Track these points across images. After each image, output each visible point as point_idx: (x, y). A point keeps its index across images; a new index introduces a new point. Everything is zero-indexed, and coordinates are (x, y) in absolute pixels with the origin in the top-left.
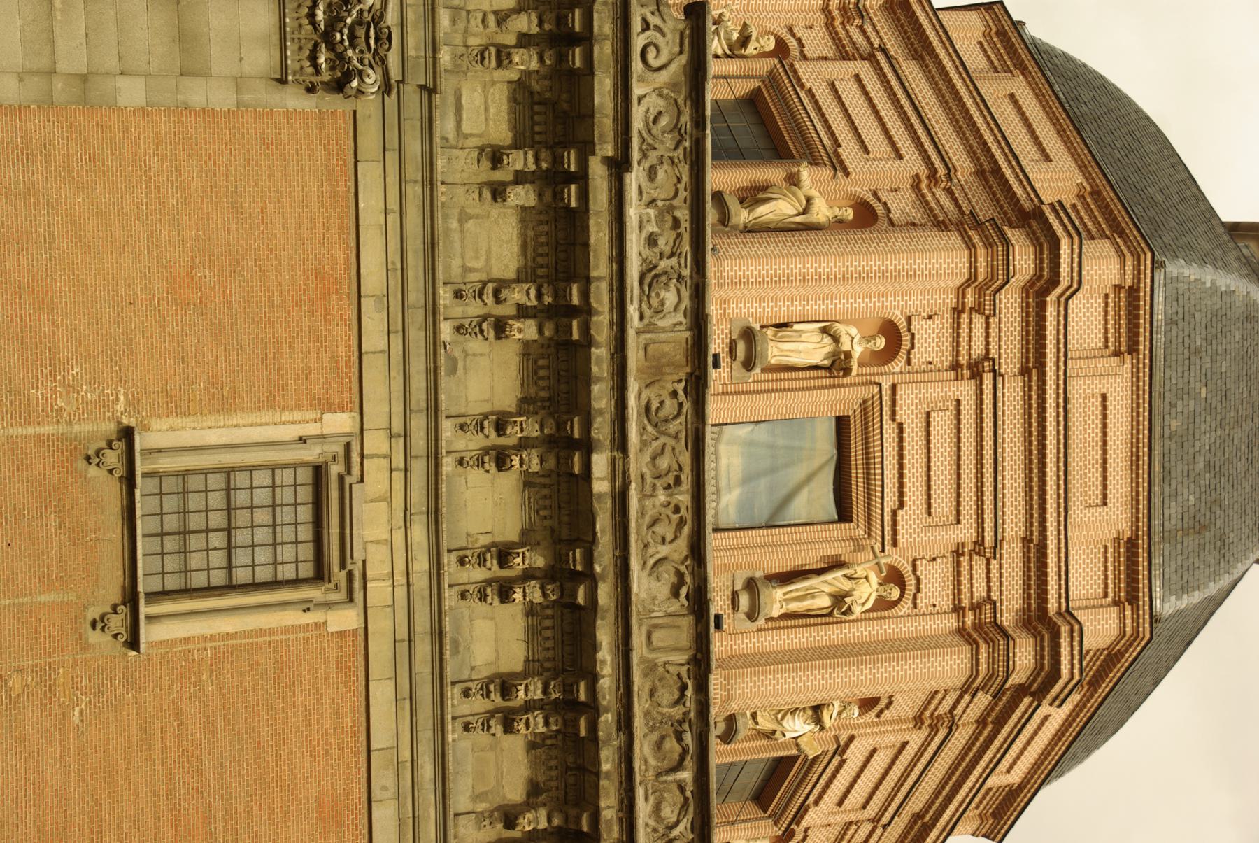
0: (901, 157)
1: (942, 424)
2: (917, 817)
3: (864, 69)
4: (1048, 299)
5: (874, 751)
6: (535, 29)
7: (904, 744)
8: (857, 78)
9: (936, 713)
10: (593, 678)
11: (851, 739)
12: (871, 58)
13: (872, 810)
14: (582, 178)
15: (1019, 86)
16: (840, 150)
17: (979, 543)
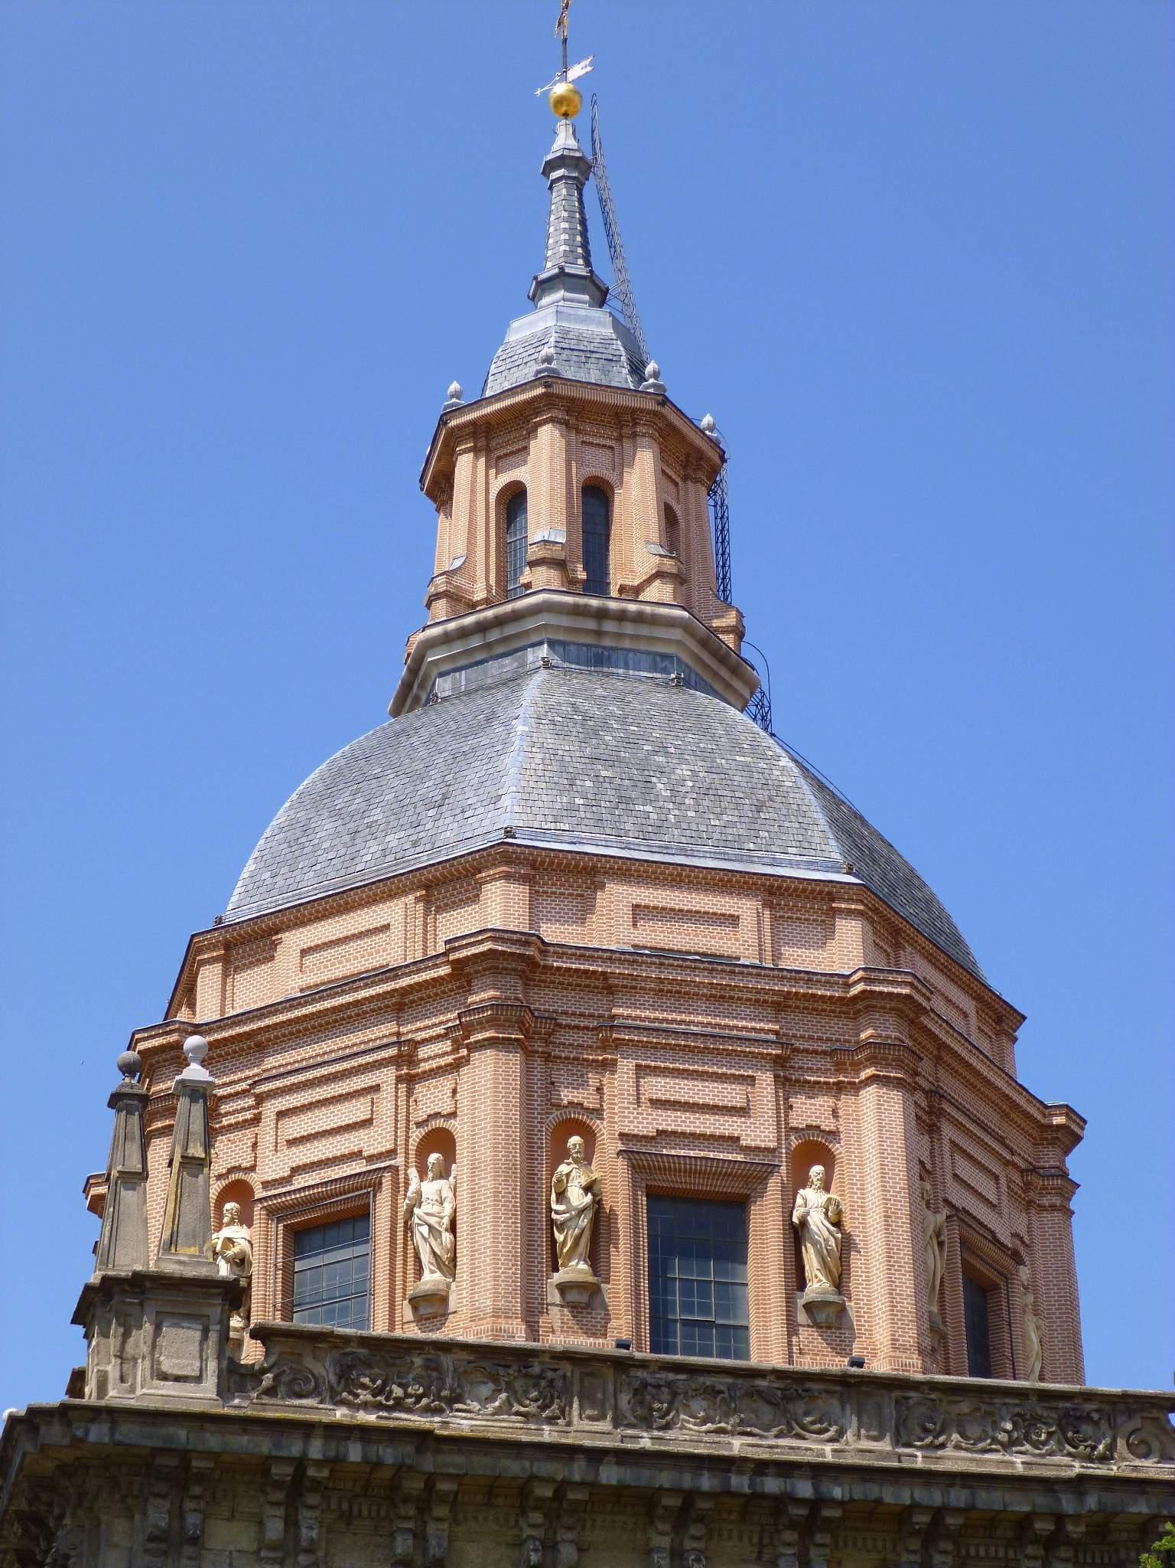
0: (376, 1088)
1: (659, 1087)
2: (1005, 1116)
3: (270, 1108)
4: (542, 963)
5: (955, 1175)
6: (280, 1512)
7: (952, 1142)
8: (281, 1115)
9: (927, 1109)
10: (914, 1507)
11: (946, 1201)
12: (260, 1099)
13: (996, 1168)
14: (430, 1480)
15: (293, 941)
16: (365, 1154)
17: (779, 1062)
